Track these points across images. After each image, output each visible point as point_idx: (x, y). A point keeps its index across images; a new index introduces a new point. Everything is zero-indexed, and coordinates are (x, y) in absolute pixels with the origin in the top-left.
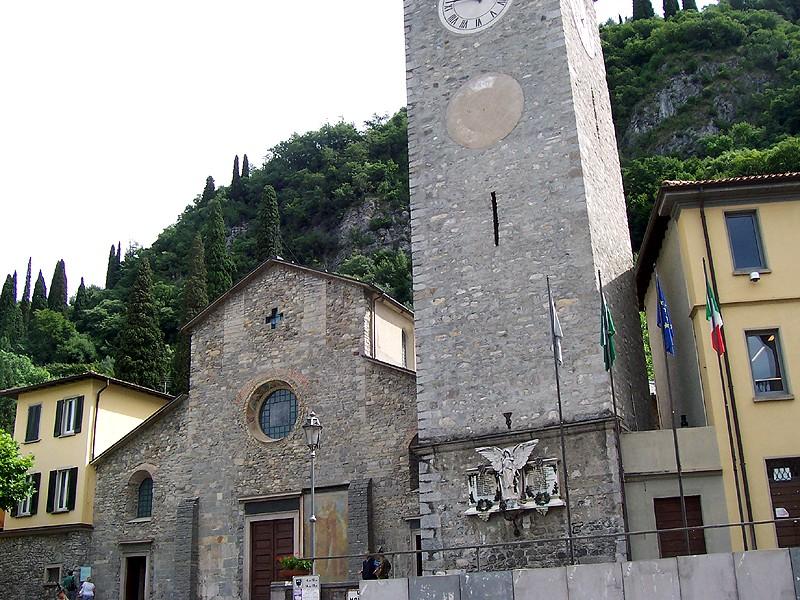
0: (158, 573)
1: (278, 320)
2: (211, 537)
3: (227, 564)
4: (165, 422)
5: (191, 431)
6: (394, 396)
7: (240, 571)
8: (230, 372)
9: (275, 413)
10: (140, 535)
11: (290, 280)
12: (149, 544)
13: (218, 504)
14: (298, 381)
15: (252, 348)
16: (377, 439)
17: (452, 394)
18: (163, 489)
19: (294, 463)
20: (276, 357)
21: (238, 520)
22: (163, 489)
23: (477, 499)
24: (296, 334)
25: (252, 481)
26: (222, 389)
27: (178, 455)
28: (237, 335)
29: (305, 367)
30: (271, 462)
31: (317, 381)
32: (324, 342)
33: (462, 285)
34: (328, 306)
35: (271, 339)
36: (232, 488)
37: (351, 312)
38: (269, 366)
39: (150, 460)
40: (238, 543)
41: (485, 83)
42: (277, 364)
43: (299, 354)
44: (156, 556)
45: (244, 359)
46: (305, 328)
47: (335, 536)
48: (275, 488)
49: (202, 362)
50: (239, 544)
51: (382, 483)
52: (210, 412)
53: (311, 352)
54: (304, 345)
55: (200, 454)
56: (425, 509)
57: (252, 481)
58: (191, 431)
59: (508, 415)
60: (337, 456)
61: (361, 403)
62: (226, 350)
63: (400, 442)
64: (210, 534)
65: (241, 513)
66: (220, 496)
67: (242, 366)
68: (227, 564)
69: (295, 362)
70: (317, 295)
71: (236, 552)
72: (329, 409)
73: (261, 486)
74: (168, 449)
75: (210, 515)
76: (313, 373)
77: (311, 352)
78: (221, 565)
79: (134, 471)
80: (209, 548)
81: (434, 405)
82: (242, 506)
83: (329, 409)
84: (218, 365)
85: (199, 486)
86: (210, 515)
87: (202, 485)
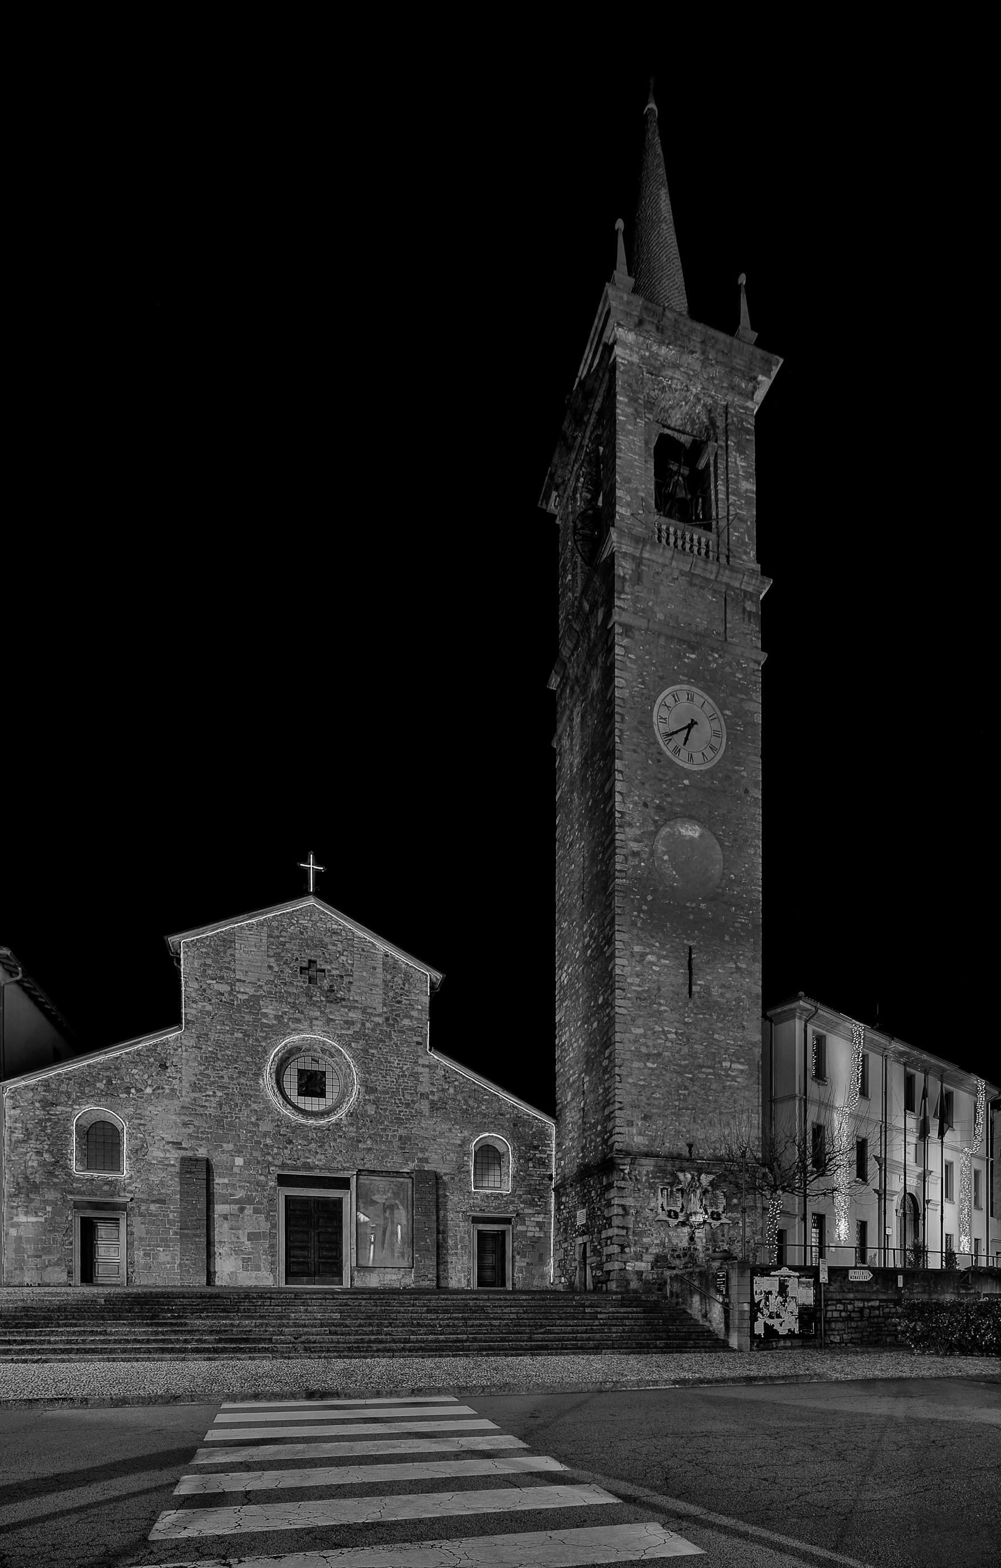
2: (227, 1206)
13: (236, 1170)
19: (344, 1141)
43: (349, 1023)
53: (363, 1024)
54: (353, 1015)
60: (396, 1143)
66: (239, 1161)
71: (265, 1226)
72: (386, 1093)
78: (244, 1239)
80: (225, 1217)
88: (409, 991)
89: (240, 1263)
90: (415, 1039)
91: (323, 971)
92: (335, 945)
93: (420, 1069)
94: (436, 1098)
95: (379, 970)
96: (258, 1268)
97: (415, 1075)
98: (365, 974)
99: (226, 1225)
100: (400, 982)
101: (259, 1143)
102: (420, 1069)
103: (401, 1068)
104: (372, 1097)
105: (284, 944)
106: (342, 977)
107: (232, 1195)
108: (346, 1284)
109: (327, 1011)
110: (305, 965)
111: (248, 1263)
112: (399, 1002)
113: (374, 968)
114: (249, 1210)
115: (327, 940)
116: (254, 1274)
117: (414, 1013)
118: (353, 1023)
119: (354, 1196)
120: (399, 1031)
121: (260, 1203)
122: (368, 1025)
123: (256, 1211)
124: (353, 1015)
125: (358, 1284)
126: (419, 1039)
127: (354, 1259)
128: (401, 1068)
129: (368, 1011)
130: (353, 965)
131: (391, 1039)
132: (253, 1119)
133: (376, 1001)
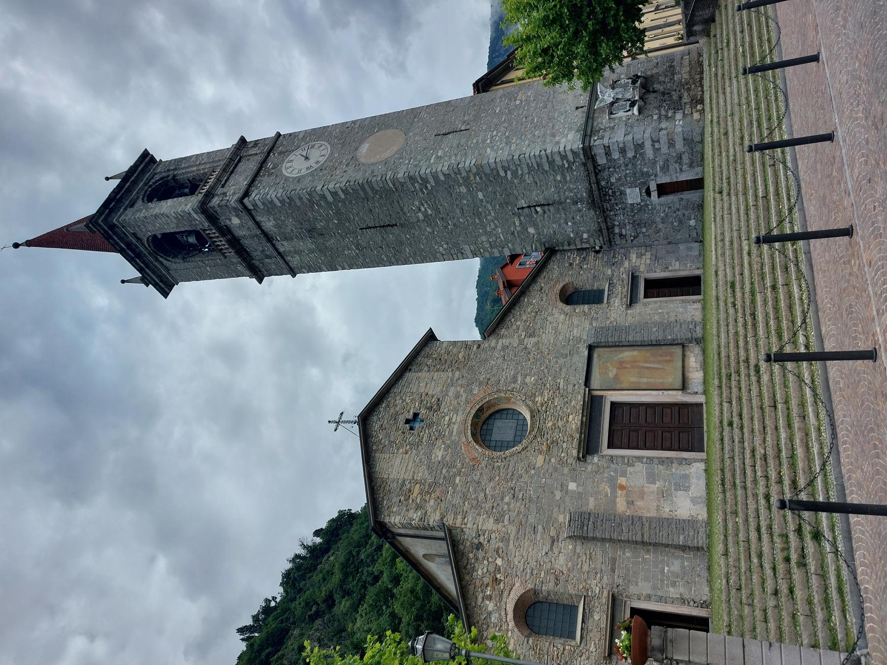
0: (655, 588)
1: (417, 425)
2: (618, 500)
3: (652, 478)
4: (465, 568)
5: (490, 525)
6: (524, 318)
7: (662, 461)
8: (444, 471)
9: (502, 429)
10: (600, 617)
11: (388, 406)
12: (615, 601)
13: (581, 489)
14: (479, 395)
15: (432, 445)
16: (556, 329)
17: (553, 135)
18: (547, 572)
19: (557, 400)
20: (450, 419)
21: (604, 463)
22: (547, 572)
23: (628, 108)
25: (565, 445)
26: (457, 481)
27: (511, 546)
28: (410, 464)
30: (550, 424)
31: (489, 379)
32: (457, 374)
33: (484, 141)
34: (429, 371)
35: (430, 426)
36: (566, 470)
37: (443, 351)
38: (456, 427)
39: (505, 594)
40: (629, 464)
41: (364, 148)
42: (458, 418)
43: (457, 396)
44: (632, 589)
45: (439, 454)
47: (634, 362)
48: (575, 421)
49: (418, 507)
50: (630, 462)
51: (594, 325)
52: (477, 499)
54: (452, 392)
55: (519, 513)
56: (630, 137)
57: (565, 445)
58: (490, 525)
59: (577, 108)
60: (561, 361)
61: (521, 342)
62: (418, 477)
63: (563, 312)
64: (615, 502)
65: (596, 459)
66: (572, 486)
67: (443, 457)
68: (652, 478)
69: (463, 399)
71: (639, 466)
72: (516, 368)
73: (572, 436)
74: (499, 562)
75: (592, 500)
76: (481, 383)
77: (461, 386)
79: (512, 624)
80: (630, 503)
81: (558, 143)
82: (589, 458)
83: (516, 368)
84: (430, 486)
85: (554, 515)
86: (592, 500)
87: (556, 509)
89: (680, 493)
91: (416, 415)
94: (523, 334)
96: (686, 477)
99: (639, 503)
101: (556, 469)
104: (519, 378)
105: (391, 442)
107: (607, 495)
108: (701, 399)
109: (446, 411)
111: (682, 484)
114: (622, 481)
116: (694, 481)
119: (610, 392)
121: (615, 471)
123: (624, 474)
124: (452, 392)
125: (700, 389)
127: (674, 392)
132: (533, 472)
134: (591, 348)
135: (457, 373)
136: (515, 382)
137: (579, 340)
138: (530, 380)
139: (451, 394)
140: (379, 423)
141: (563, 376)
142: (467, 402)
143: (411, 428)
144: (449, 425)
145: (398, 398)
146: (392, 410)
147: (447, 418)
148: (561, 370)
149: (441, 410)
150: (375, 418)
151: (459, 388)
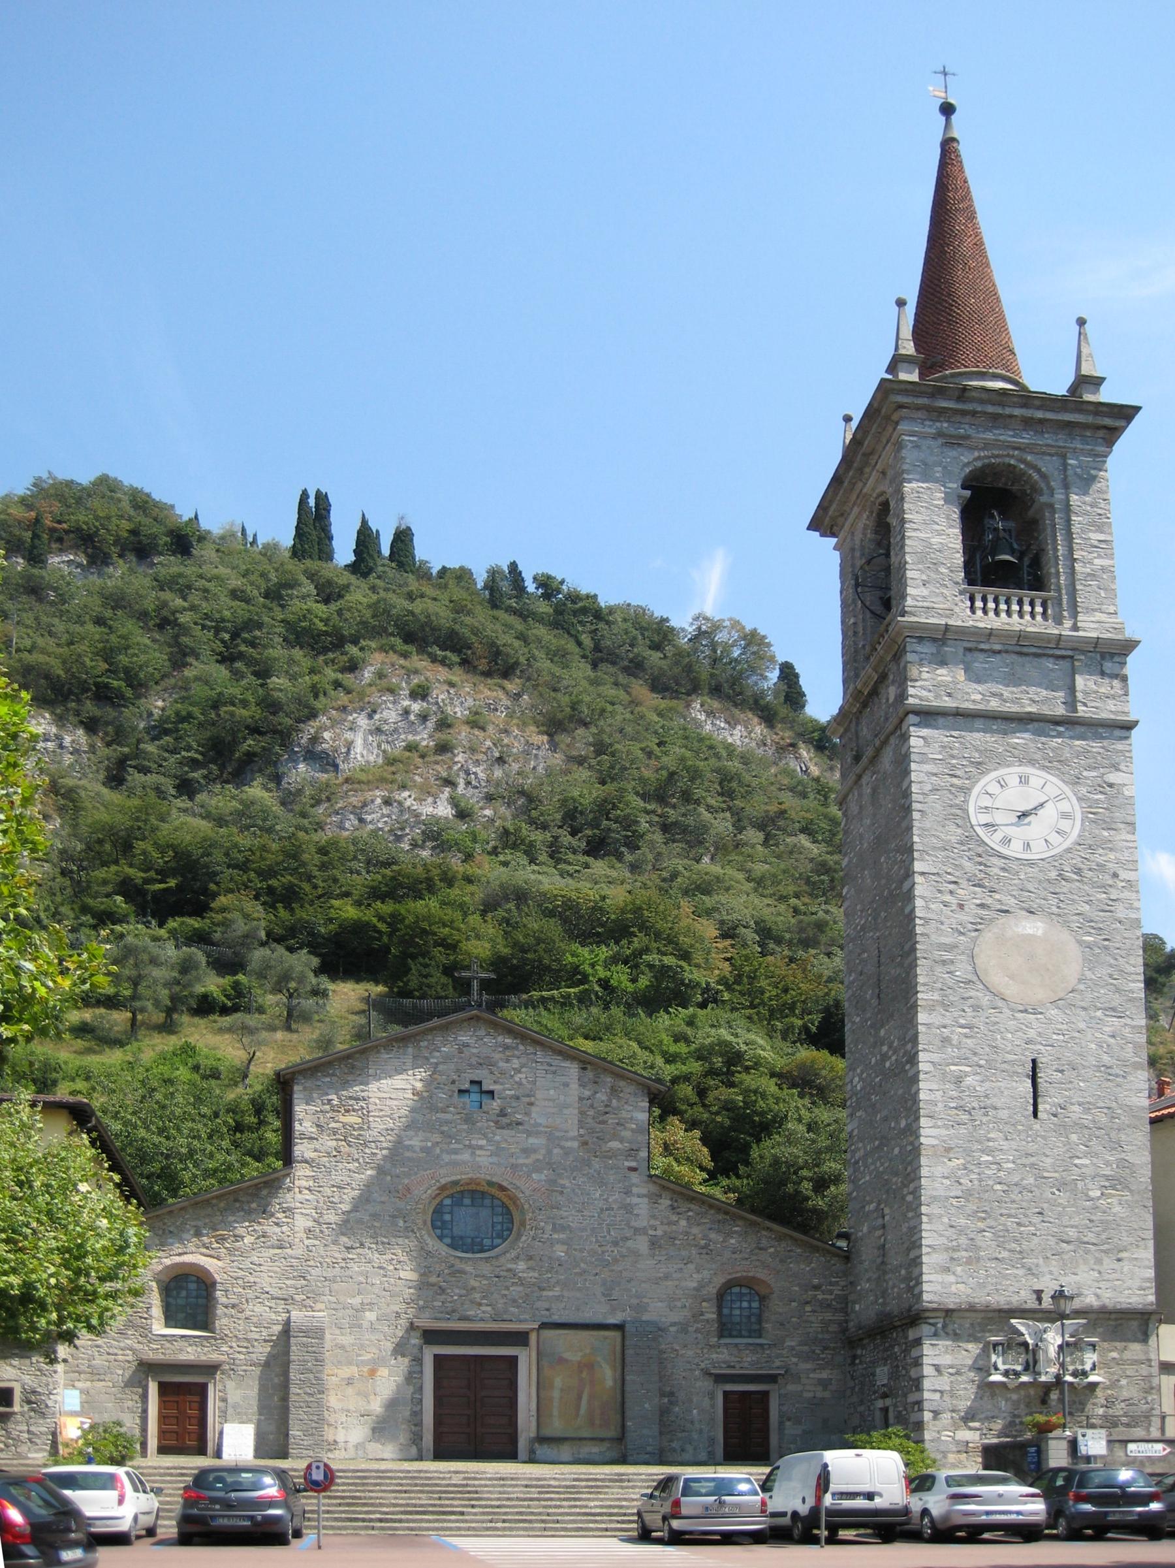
1: (475, 1097)
14: (528, 1186)
20: (481, 1148)
24: (518, 1124)
29: (538, 1170)
43: (526, 1151)
46: (538, 1116)
53: (549, 1152)
69: (521, 1161)
70: (564, 1079)
72: (584, 1230)
76: (552, 1182)
77: (549, 1152)
83: (584, 1230)
88: (618, 1108)
90: (627, 1164)
92: (507, 1061)
93: (635, 1200)
95: (574, 1086)
97: (628, 1209)
98: (552, 1092)
100: (604, 1098)
102: (635, 1200)
103: (606, 1200)
106: (518, 1098)
109: (498, 1138)
110: (467, 1086)
112: (604, 1122)
113: (566, 1085)
115: (497, 1056)
117: (627, 1134)
118: (535, 1151)
120: (605, 1157)
122: (556, 1151)
126: (633, 1164)
128: (606, 1200)
129: (557, 1134)
130: (534, 1083)
131: (589, 1166)
133: (569, 1123)
134: (620, 1327)
135: (575, 1144)
136: (554, 1230)
137: (640, 1308)
138: (560, 1252)
139: (531, 1140)
140: (472, 1041)
141: (566, 1294)
142: (514, 1167)
143: (461, 1092)
144: (470, 1146)
145: (523, 1060)
146: (497, 1056)
147: (484, 1142)
148: (579, 1289)
149: (499, 1131)
150: (482, 1032)
151: (543, 1152)
